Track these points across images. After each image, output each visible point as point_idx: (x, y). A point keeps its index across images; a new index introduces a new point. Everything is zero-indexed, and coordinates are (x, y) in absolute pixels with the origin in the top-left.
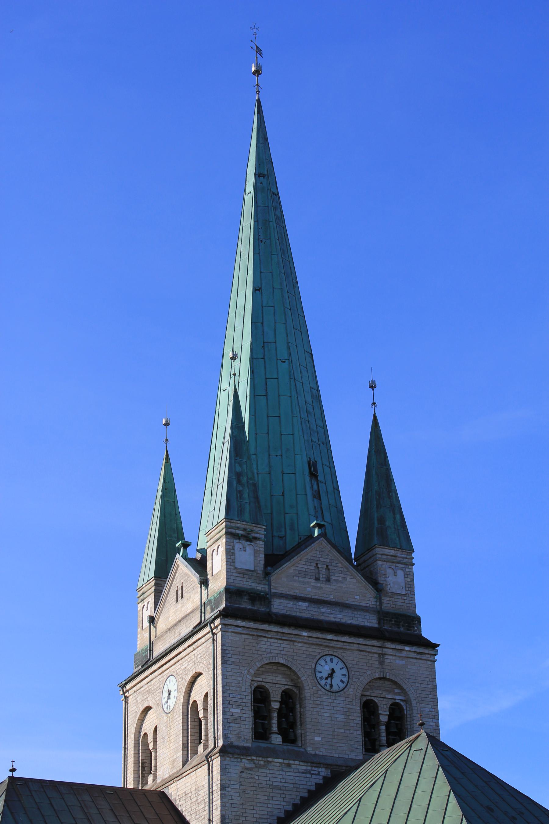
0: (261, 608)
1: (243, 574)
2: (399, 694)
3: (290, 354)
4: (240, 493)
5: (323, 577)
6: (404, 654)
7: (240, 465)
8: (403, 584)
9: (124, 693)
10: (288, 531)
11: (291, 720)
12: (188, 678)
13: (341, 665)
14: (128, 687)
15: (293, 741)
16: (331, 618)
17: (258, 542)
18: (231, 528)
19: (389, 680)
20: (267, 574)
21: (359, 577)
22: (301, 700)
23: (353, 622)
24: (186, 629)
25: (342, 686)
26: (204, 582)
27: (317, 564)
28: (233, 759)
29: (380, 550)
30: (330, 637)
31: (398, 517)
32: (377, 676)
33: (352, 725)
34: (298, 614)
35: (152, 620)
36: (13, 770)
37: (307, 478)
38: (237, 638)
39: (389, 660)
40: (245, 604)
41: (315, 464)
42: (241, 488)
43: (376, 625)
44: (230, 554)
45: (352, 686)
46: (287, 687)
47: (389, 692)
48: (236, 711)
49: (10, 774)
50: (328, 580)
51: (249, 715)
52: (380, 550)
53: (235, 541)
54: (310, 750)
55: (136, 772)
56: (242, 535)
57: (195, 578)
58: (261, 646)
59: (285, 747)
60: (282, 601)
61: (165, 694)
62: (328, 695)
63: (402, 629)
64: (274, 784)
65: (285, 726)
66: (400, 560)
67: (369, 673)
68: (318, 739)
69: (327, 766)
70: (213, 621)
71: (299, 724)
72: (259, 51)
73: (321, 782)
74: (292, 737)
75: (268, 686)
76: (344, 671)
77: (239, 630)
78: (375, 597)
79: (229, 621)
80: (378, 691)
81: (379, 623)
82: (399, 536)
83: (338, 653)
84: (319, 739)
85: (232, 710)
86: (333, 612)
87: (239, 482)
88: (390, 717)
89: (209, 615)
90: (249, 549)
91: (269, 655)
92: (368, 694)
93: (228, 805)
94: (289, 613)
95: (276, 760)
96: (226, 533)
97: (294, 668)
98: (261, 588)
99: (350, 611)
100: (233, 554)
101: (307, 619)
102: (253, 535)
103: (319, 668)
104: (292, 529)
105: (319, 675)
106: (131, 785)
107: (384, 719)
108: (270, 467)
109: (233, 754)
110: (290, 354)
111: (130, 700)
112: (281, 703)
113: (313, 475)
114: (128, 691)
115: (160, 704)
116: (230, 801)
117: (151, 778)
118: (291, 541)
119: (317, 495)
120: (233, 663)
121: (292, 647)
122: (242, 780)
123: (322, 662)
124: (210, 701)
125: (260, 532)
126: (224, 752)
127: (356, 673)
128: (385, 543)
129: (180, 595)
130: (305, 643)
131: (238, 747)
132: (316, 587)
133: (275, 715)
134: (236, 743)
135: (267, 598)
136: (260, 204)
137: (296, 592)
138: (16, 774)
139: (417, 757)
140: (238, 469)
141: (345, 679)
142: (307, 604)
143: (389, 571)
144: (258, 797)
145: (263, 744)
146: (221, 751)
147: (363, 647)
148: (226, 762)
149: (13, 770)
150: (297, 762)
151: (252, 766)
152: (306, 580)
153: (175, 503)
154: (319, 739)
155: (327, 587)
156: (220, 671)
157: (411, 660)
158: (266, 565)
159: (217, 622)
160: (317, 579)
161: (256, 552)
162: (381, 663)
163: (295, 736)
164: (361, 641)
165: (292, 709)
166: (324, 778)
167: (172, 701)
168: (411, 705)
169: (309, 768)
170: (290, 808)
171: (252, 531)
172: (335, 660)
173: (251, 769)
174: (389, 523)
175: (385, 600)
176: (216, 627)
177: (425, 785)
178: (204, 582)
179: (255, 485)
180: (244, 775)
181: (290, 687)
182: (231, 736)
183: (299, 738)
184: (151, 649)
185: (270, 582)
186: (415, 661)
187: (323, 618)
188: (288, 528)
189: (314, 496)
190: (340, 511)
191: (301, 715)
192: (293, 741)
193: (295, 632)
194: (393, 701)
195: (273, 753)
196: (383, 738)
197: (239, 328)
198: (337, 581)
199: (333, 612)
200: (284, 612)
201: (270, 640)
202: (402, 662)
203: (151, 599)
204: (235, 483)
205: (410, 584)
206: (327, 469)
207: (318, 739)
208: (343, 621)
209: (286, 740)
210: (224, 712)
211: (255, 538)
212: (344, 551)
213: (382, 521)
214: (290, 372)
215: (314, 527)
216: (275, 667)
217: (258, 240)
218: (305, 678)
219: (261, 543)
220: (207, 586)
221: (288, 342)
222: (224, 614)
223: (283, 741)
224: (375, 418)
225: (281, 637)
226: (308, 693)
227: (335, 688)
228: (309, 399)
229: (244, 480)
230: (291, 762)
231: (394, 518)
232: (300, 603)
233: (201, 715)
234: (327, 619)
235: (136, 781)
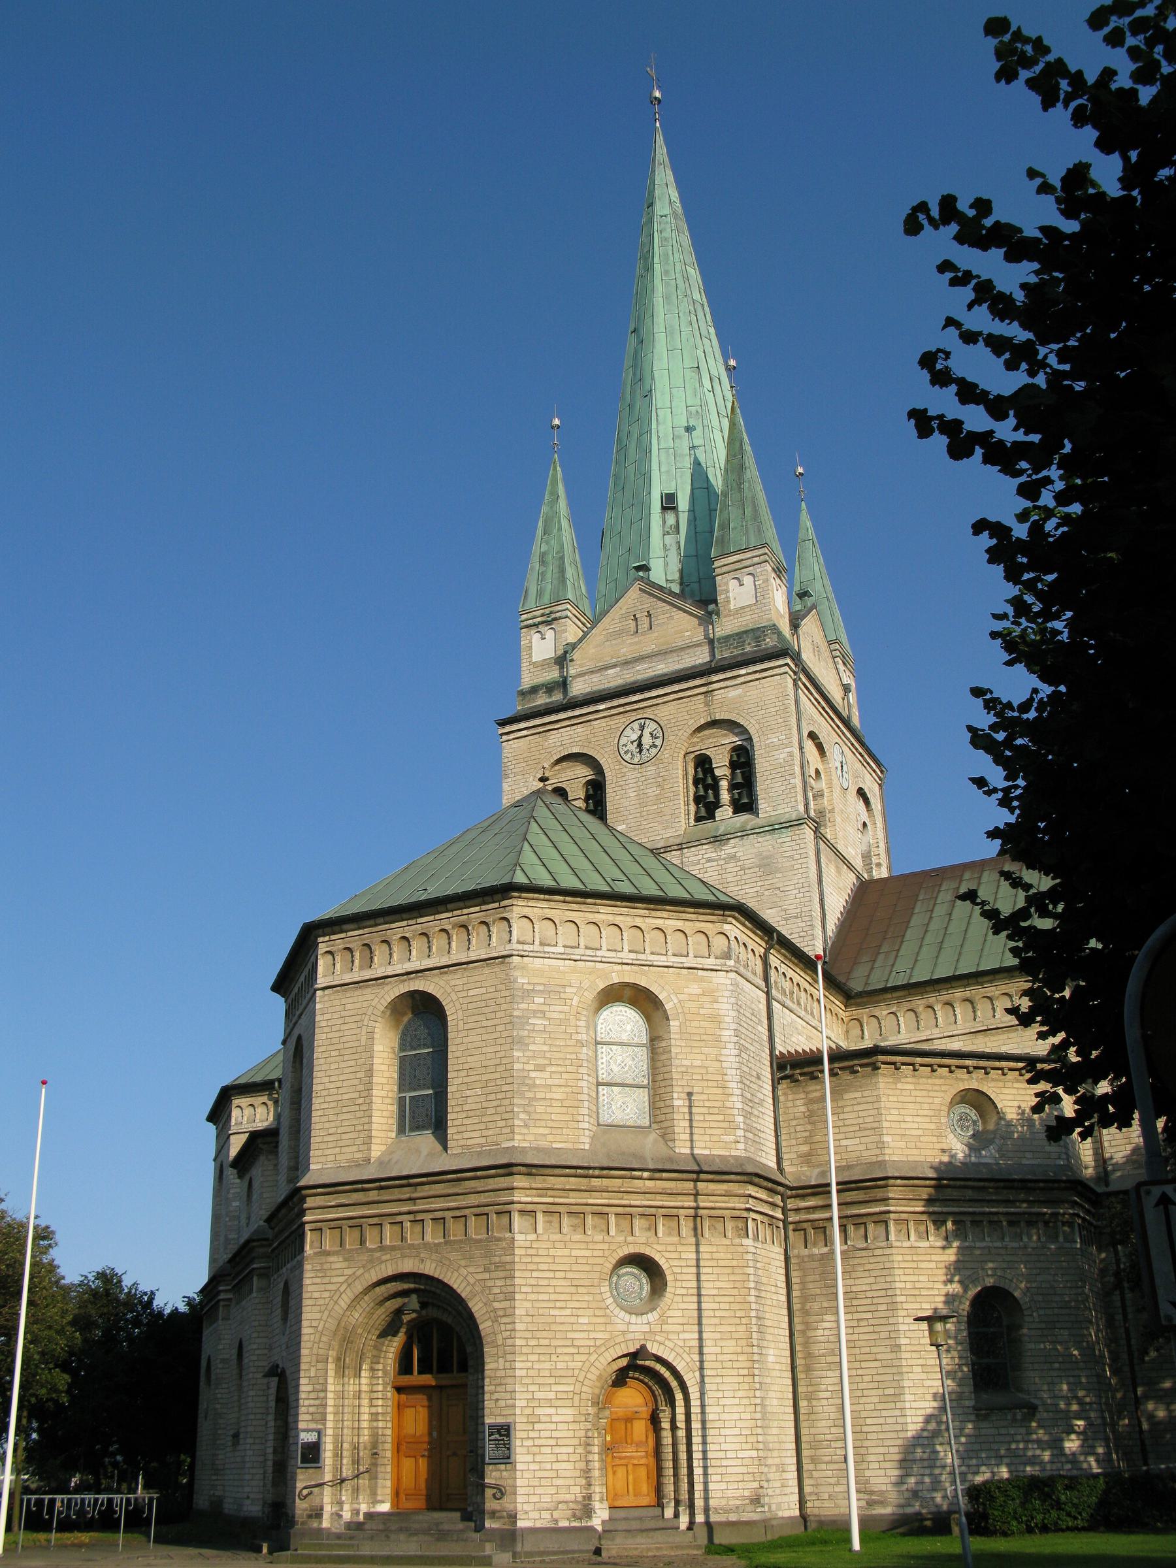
0: (557, 697)
27: (634, 616)
32: (703, 722)
33: (668, 795)
34: (607, 686)
45: (668, 747)
58: (551, 741)
62: (635, 769)
80: (711, 740)
86: (651, 665)
120: (516, 774)
121: (589, 728)
127: (673, 729)
157: (751, 684)
181: (593, 777)
186: (757, 682)
187: (639, 677)
194: (733, 745)
199: (651, 665)
200: (589, 690)
201: (560, 731)
208: (665, 671)
225: (573, 722)
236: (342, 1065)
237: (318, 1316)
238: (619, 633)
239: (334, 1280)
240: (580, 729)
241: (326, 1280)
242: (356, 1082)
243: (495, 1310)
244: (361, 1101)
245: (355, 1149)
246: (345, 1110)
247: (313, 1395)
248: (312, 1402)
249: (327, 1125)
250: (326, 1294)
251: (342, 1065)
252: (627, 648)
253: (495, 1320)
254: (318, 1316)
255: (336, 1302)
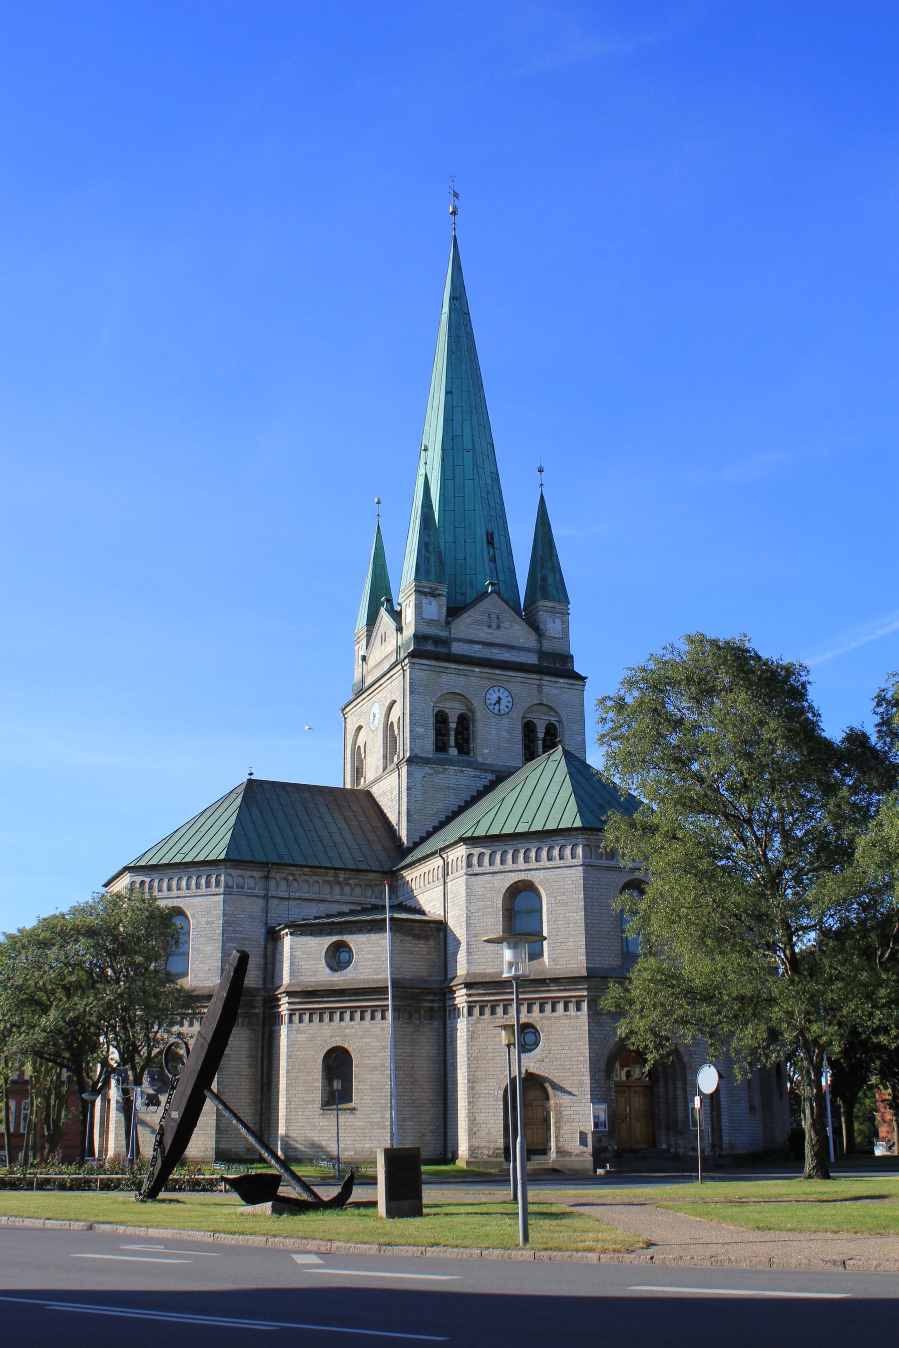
0: (444, 650)
1: (429, 623)
2: (554, 716)
3: (474, 445)
4: (428, 558)
5: (494, 625)
6: (558, 685)
7: (428, 536)
8: (560, 630)
9: (344, 715)
10: (468, 588)
11: (466, 736)
12: (387, 704)
13: (507, 694)
14: (347, 710)
15: (467, 753)
16: (500, 657)
17: (441, 598)
18: (419, 586)
19: (546, 705)
20: (448, 623)
21: (524, 624)
22: (474, 721)
23: (518, 660)
24: (386, 666)
25: (507, 710)
26: (400, 629)
28: (417, 767)
29: (542, 603)
30: (498, 672)
31: (558, 576)
34: (473, 654)
35: (364, 658)
36: (251, 774)
37: (485, 546)
38: (422, 673)
39: (546, 689)
40: (430, 647)
41: (492, 535)
42: (428, 555)
43: (537, 663)
44: (418, 607)
46: (462, 711)
47: (545, 714)
48: (421, 730)
49: (249, 777)
50: (499, 627)
51: (431, 733)
52: (542, 603)
53: (423, 597)
54: (480, 759)
55: (352, 775)
56: (429, 593)
57: (393, 625)
59: (460, 758)
60: (460, 644)
61: (372, 717)
63: (558, 665)
64: (450, 785)
65: (460, 741)
66: (558, 611)
67: (529, 700)
68: (486, 751)
69: (493, 772)
70: (403, 661)
71: (471, 740)
72: (456, 195)
73: (488, 784)
74: (466, 750)
75: (447, 711)
76: (509, 699)
77: (424, 667)
78: (537, 641)
79: (416, 660)
81: (539, 661)
82: (558, 591)
83: (505, 684)
84: (488, 751)
85: (418, 729)
87: (427, 550)
88: (546, 734)
89: (402, 656)
90: (434, 602)
91: (449, 687)
92: (529, 716)
93: (413, 801)
94: (465, 653)
95: (452, 767)
96: (415, 591)
97: (468, 697)
98: (443, 634)
99: (516, 652)
100: (421, 607)
101: (480, 658)
102: (437, 592)
103: (488, 696)
104: (471, 587)
105: (488, 702)
106: (348, 786)
107: (541, 735)
108: (455, 537)
109: (417, 763)
110: (474, 445)
111: (348, 720)
112: (457, 723)
113: (490, 543)
114: (346, 713)
115: (368, 724)
116: (415, 799)
117: (362, 780)
118: (470, 596)
119: (493, 560)
122: (424, 783)
123: (491, 691)
124: (401, 723)
125: (444, 589)
126: (410, 761)
128: (546, 597)
129: (384, 639)
130: (477, 677)
131: (421, 758)
132: (487, 633)
133: (453, 733)
134: (420, 755)
135: (448, 642)
136: (453, 322)
137: (472, 637)
138: (253, 777)
139: (551, 766)
140: (427, 540)
141: (510, 705)
142: (480, 647)
143: (549, 620)
144: (437, 795)
145: (442, 755)
146: (406, 761)
147: (524, 680)
148: (411, 769)
149: (251, 774)
150: (468, 769)
151: (432, 772)
152: (480, 627)
153: (384, 566)
154: (488, 751)
155: (497, 633)
156: (408, 700)
157: (565, 690)
158: (447, 616)
159: (407, 661)
160: (490, 626)
161: (440, 606)
162: (540, 692)
163: (469, 748)
164: (523, 675)
165: (467, 729)
166: (490, 781)
167: (376, 721)
168: (563, 724)
169: (478, 773)
170: (462, 804)
171: (436, 589)
172: (502, 690)
173: (431, 774)
174: (550, 580)
175: (545, 642)
176: (406, 665)
177: (554, 787)
178: (400, 629)
179: (440, 552)
180: (425, 779)
182: (416, 749)
183: (472, 750)
184: (363, 682)
185: (450, 629)
187: (493, 657)
188: (468, 586)
189: (490, 560)
190: (513, 572)
191: (473, 732)
192: (467, 753)
193: (470, 668)
195: (450, 762)
196: (540, 750)
197: (434, 424)
198: (506, 628)
200: (461, 653)
202: (557, 691)
203: (364, 642)
204: (423, 551)
205: (566, 630)
206: (502, 538)
207: (486, 751)
208: (510, 659)
209: (461, 752)
210: (411, 731)
211: (439, 595)
212: (513, 604)
213: (544, 579)
214: (473, 459)
215: (488, 585)
216: (453, 696)
217: (451, 352)
218: (477, 704)
219: (444, 598)
220: (401, 633)
221: (473, 436)
222: (412, 655)
223: (459, 753)
224: (542, 496)
225: (458, 673)
226: (479, 716)
227: (502, 712)
228: (489, 481)
229: (431, 548)
230: (464, 769)
231: (555, 577)
232: (475, 646)
233: (396, 733)
234: (497, 658)
235: (352, 783)
236: (601, 911)
237: (598, 1047)
238: (479, 623)
239: (605, 1028)
240: (462, 679)
241: (601, 1028)
242: (610, 922)
243: (690, 1051)
244: (613, 933)
245: (611, 959)
246: (604, 936)
247: (597, 1089)
248: (597, 1093)
249: (594, 943)
250: (602, 1036)
251: (601, 911)
252: (484, 634)
253: (691, 1056)
254: (598, 1047)
255: (608, 1041)
